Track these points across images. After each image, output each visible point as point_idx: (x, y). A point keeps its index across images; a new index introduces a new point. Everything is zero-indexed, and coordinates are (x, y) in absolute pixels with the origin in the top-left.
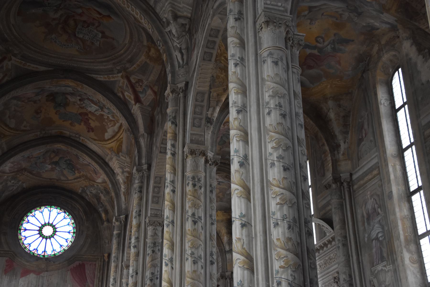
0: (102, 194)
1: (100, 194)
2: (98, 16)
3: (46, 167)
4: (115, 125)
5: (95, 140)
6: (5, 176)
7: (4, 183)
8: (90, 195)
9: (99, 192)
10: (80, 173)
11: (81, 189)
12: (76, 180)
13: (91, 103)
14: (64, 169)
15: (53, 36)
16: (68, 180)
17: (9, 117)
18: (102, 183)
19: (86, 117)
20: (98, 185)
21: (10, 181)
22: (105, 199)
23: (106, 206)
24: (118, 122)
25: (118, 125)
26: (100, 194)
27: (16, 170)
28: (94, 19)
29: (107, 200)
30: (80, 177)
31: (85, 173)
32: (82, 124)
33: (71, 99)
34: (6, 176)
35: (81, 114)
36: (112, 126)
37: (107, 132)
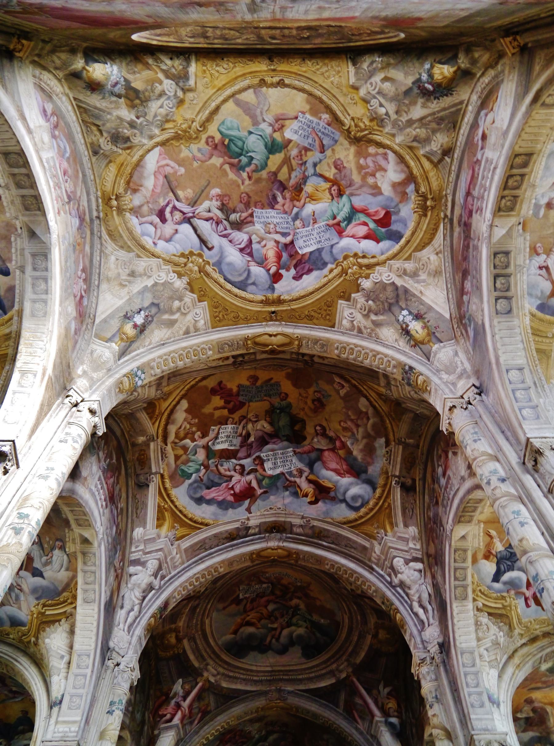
0: (129, 119)
1: (134, 118)
2: (248, 618)
3: (296, 132)
4: (177, 434)
5: (204, 378)
6: (399, 145)
7: (404, 120)
8: (161, 83)
9: (139, 121)
10: (207, 143)
11: (192, 82)
12: (213, 105)
13: (230, 448)
14: (250, 133)
15: (299, 584)
16: (233, 95)
17: (368, 419)
18: (143, 157)
19: (231, 405)
20: (151, 137)
21: (387, 114)
22: (115, 114)
23: (103, 98)
24: (173, 442)
25: (172, 437)
26: (134, 118)
27: (372, 150)
28: (252, 610)
29: (109, 113)
30: (204, 125)
31: (194, 147)
32: (235, 389)
33: (264, 425)
34: (398, 139)
35: (242, 405)
36: (180, 428)
37: (186, 411)
